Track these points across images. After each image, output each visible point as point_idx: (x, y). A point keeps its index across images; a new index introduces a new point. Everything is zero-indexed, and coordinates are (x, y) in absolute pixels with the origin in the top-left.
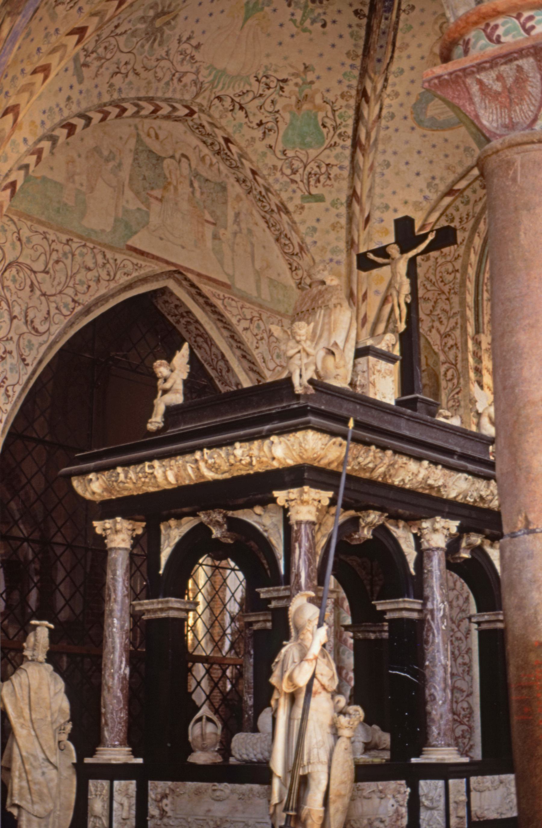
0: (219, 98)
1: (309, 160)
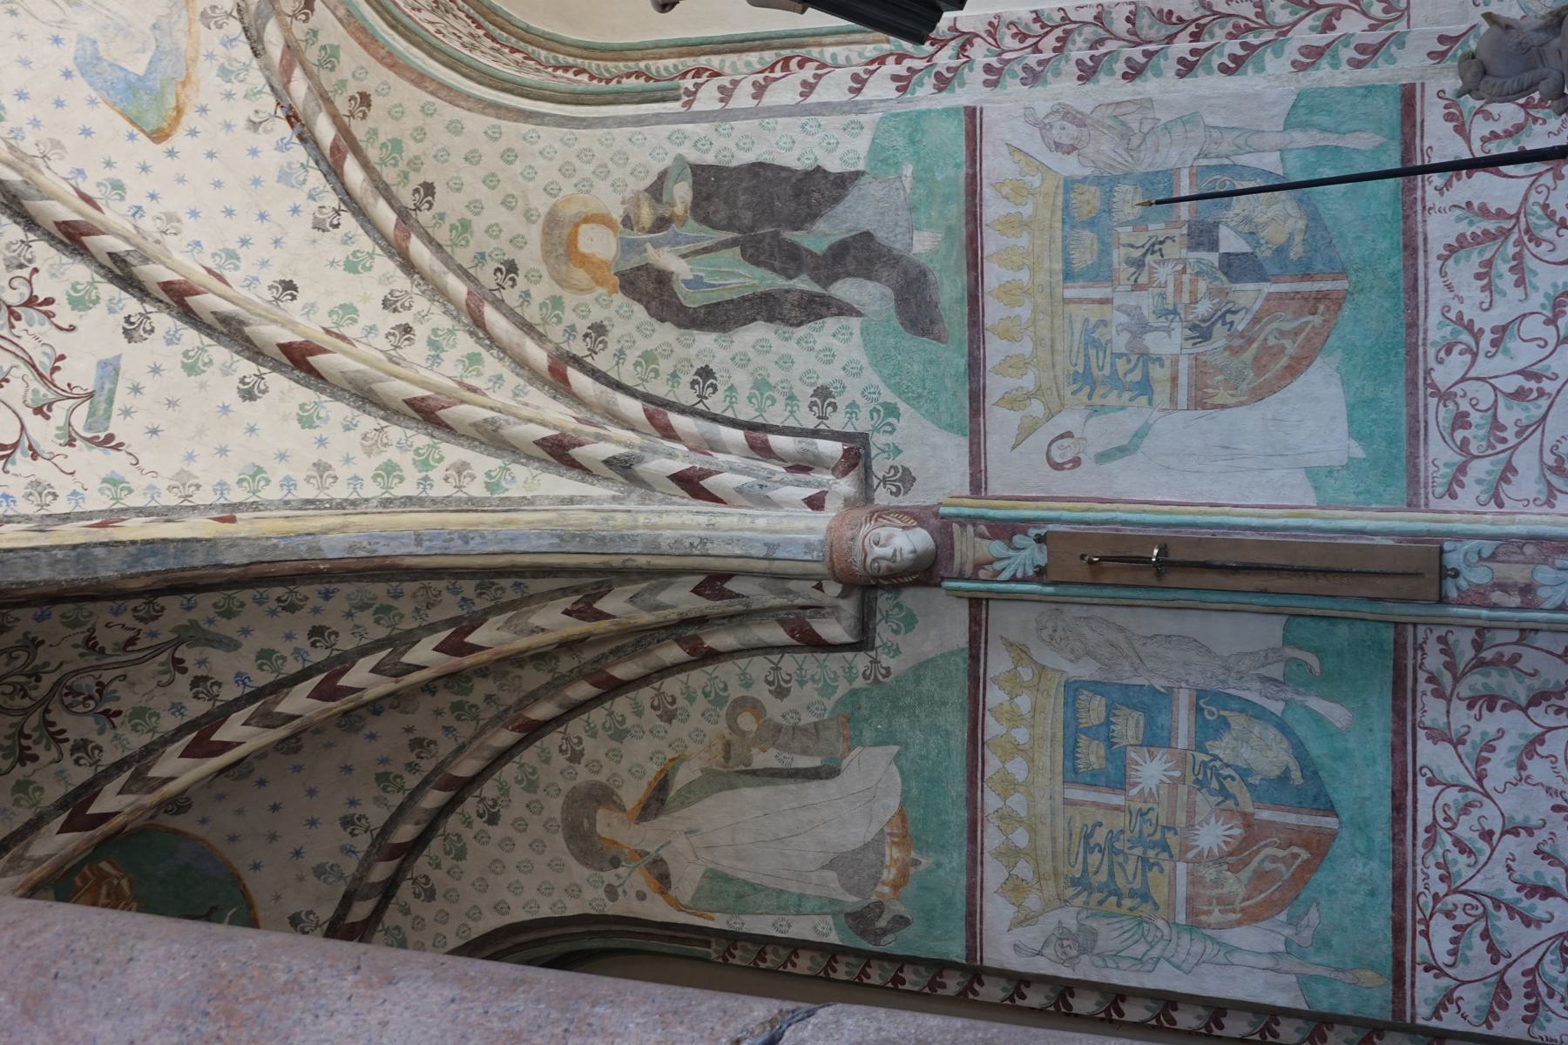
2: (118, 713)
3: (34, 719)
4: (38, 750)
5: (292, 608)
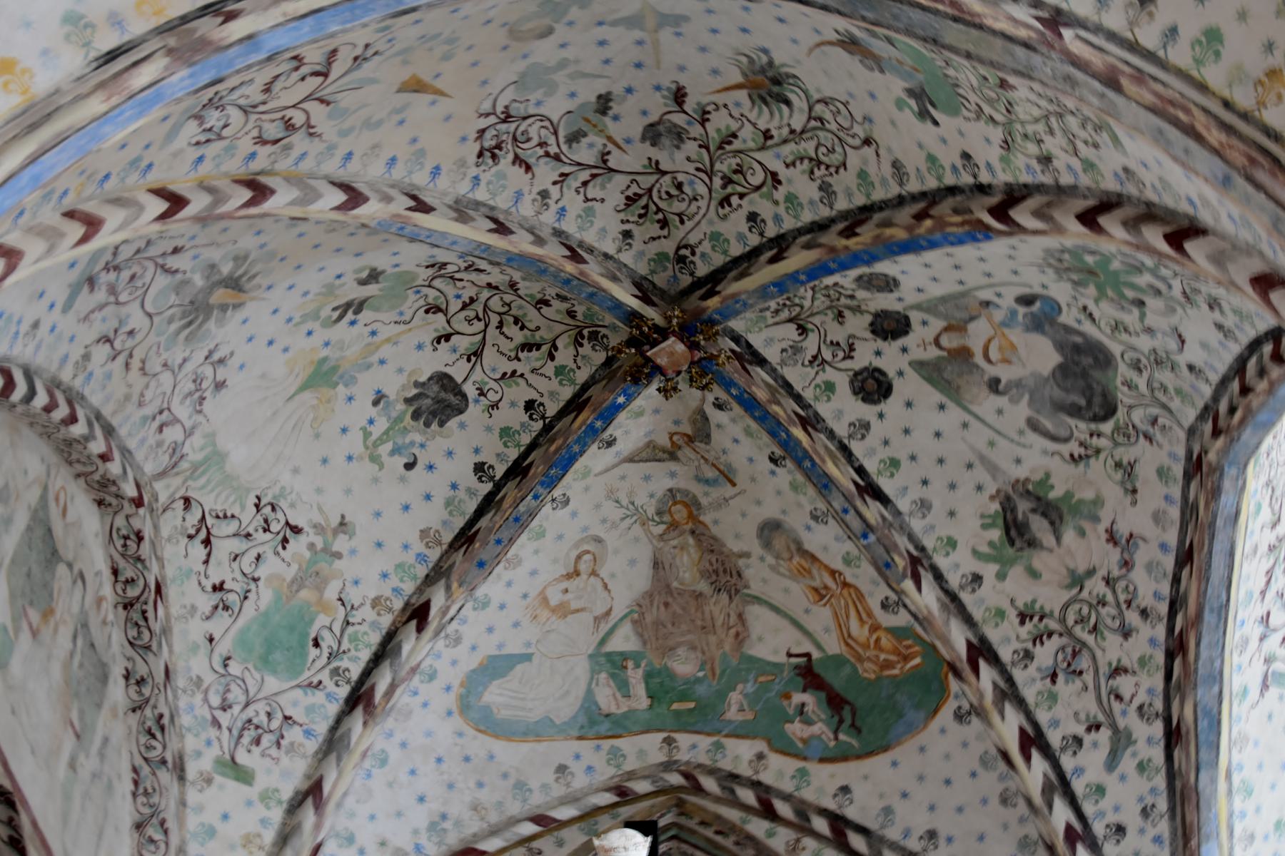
0: (187, 501)
1: (260, 696)
2: (1054, 682)
3: (1053, 625)
4: (1029, 626)
5: (1145, 813)
